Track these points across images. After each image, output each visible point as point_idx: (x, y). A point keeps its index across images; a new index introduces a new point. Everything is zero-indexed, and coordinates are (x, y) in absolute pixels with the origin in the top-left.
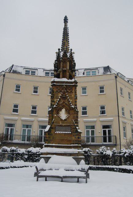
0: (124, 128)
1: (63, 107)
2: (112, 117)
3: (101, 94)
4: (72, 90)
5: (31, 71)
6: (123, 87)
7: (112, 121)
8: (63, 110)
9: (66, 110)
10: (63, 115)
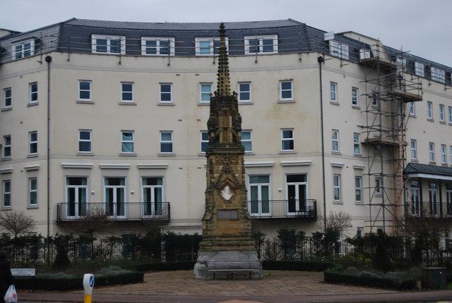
0: (337, 179)
1: (227, 184)
2: (309, 154)
5: (111, 41)
7: (307, 165)
8: (227, 188)
10: (227, 194)
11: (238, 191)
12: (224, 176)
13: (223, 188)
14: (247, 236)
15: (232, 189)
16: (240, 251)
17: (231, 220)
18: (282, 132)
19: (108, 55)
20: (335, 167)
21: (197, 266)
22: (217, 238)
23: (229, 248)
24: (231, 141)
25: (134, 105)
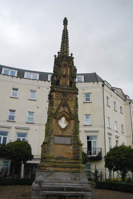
0: (110, 138)
1: (63, 115)
3: (87, 103)
4: (73, 98)
6: (109, 96)
8: (63, 119)
9: (66, 119)
10: (63, 123)
11: (72, 122)
12: (62, 109)
13: (60, 118)
14: (79, 160)
15: (67, 120)
16: (73, 172)
17: (65, 145)
18: (85, 116)
20: (110, 134)
21: (34, 183)
22: (52, 160)
23: (62, 169)
24: (68, 84)
25: (17, 98)
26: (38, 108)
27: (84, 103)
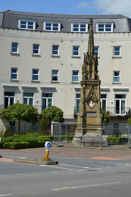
10: (91, 105)
19: (27, 30)
21: (74, 139)
23: (91, 131)
25: (40, 56)
26: (62, 65)
27: (113, 58)
